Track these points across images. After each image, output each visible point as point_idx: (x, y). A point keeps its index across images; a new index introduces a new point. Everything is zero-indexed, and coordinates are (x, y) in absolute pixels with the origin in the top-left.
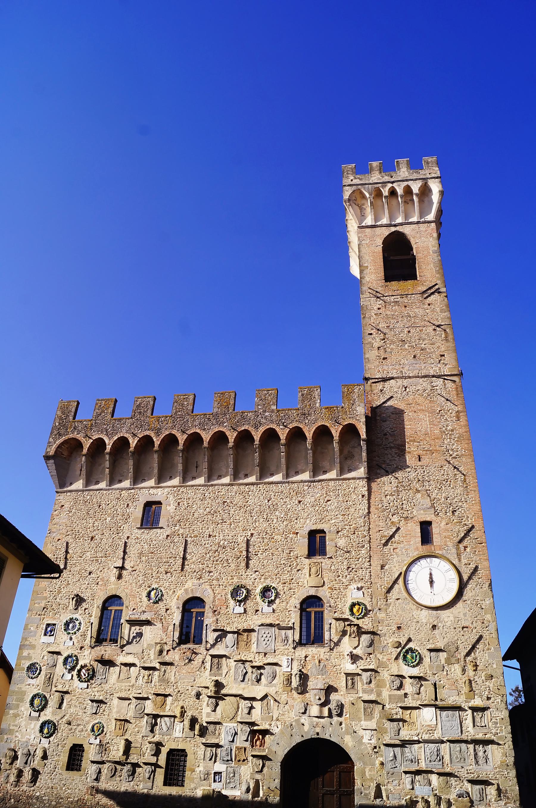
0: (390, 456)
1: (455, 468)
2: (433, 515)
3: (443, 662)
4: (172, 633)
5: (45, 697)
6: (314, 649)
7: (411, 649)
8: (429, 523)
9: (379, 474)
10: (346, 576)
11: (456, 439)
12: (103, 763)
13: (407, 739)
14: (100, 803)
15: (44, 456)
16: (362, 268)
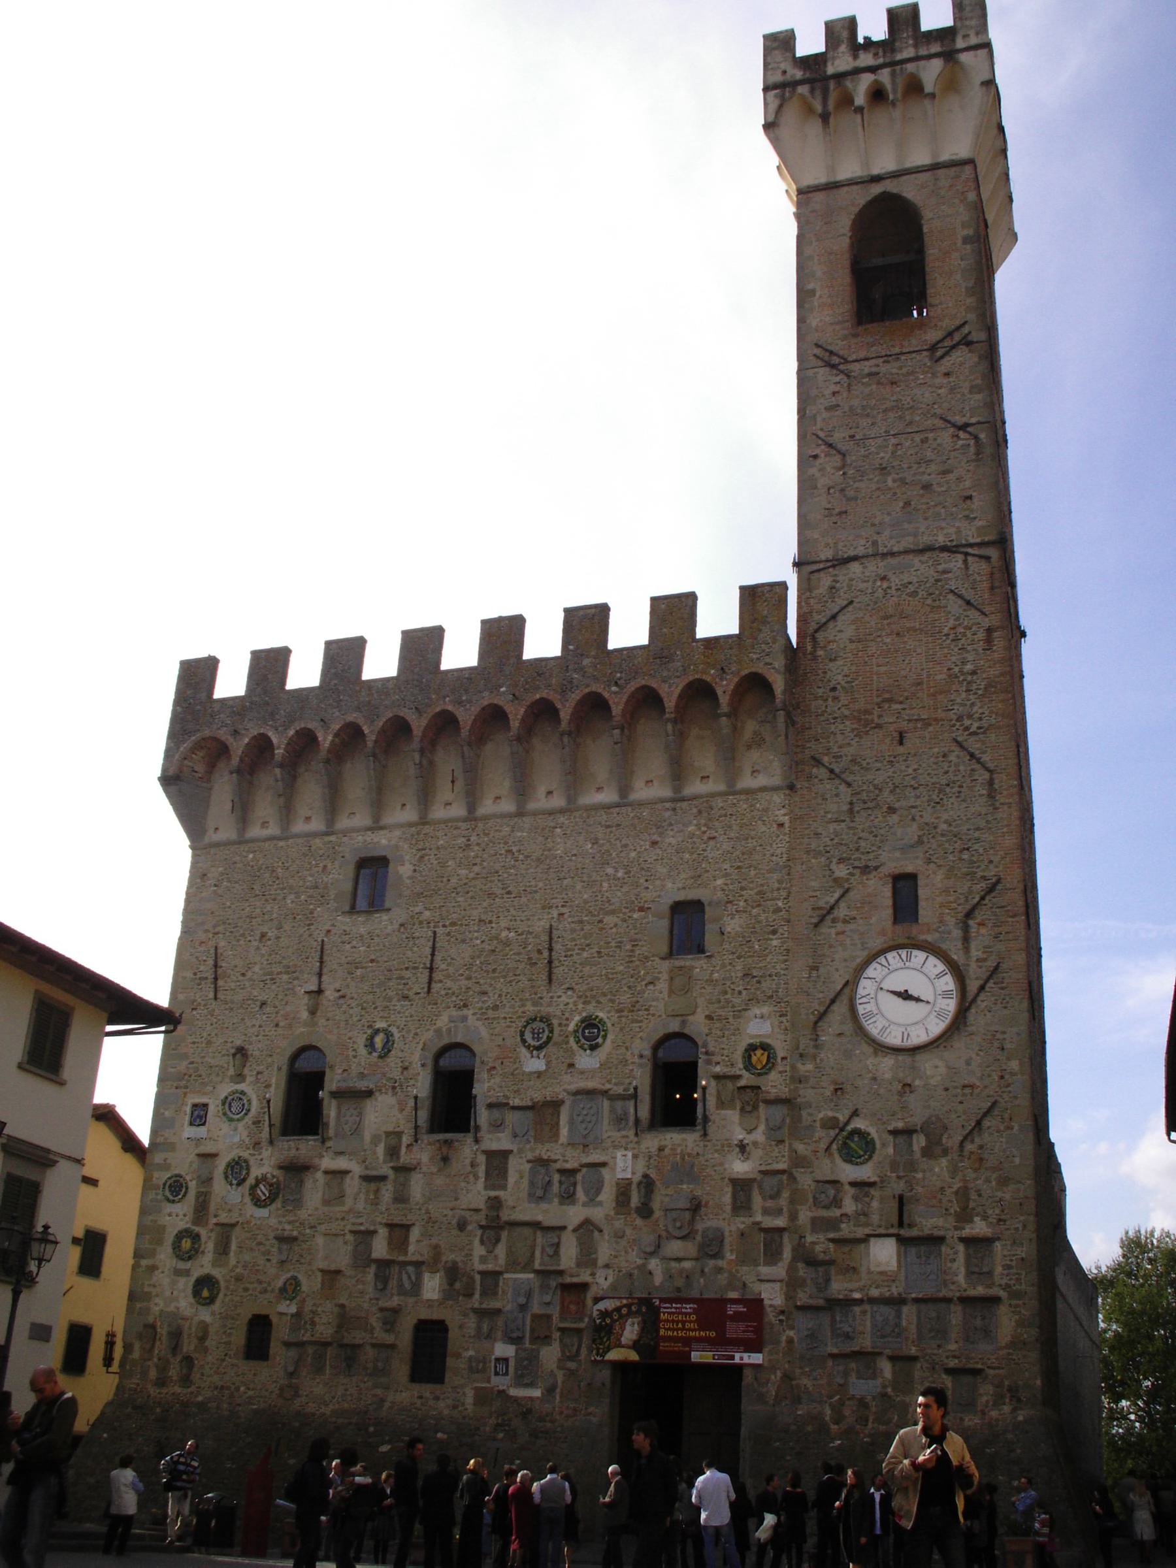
0: (840, 738)
1: (972, 755)
3: (917, 1154)
7: (857, 1132)
8: (912, 878)
10: (740, 993)
11: (980, 692)
12: (301, 1345)
13: (841, 1297)
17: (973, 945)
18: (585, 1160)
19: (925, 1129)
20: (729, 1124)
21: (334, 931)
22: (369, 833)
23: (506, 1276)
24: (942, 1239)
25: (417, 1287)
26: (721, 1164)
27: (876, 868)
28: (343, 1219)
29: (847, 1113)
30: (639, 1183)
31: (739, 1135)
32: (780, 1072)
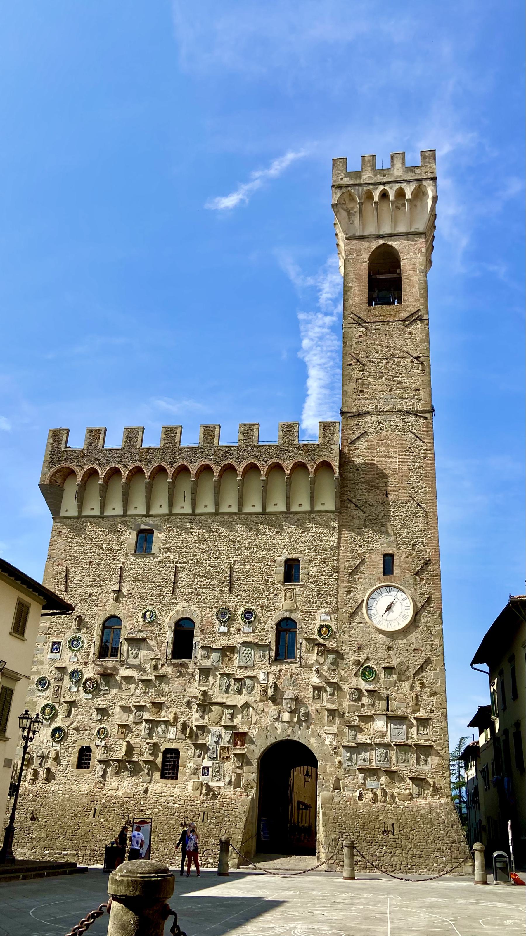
0: (360, 491)
1: (418, 505)
2: (395, 549)
4: (165, 649)
5: (54, 707)
7: (368, 667)
8: (392, 555)
10: (316, 602)
11: (422, 477)
13: (362, 742)
14: (107, 795)
15: (39, 485)
16: (346, 289)
22: (144, 518)
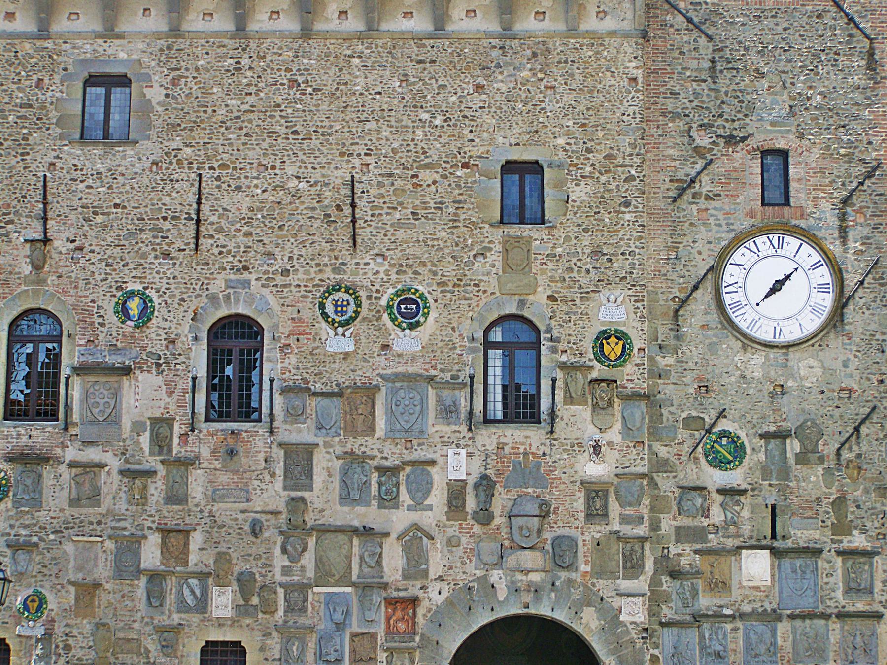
1: (851, 20)
4: (188, 396)
6: (517, 433)
7: (724, 434)
9: (672, 26)
10: (588, 271)
17: (851, 235)
18: (407, 458)
19: (798, 433)
20: (578, 421)
21: (59, 164)
22: (100, 42)
23: (316, 589)
24: (818, 552)
25: (202, 604)
26: (572, 466)
27: (744, 139)
28: (99, 523)
29: (714, 414)
30: (476, 486)
31: (591, 432)
32: (637, 365)
